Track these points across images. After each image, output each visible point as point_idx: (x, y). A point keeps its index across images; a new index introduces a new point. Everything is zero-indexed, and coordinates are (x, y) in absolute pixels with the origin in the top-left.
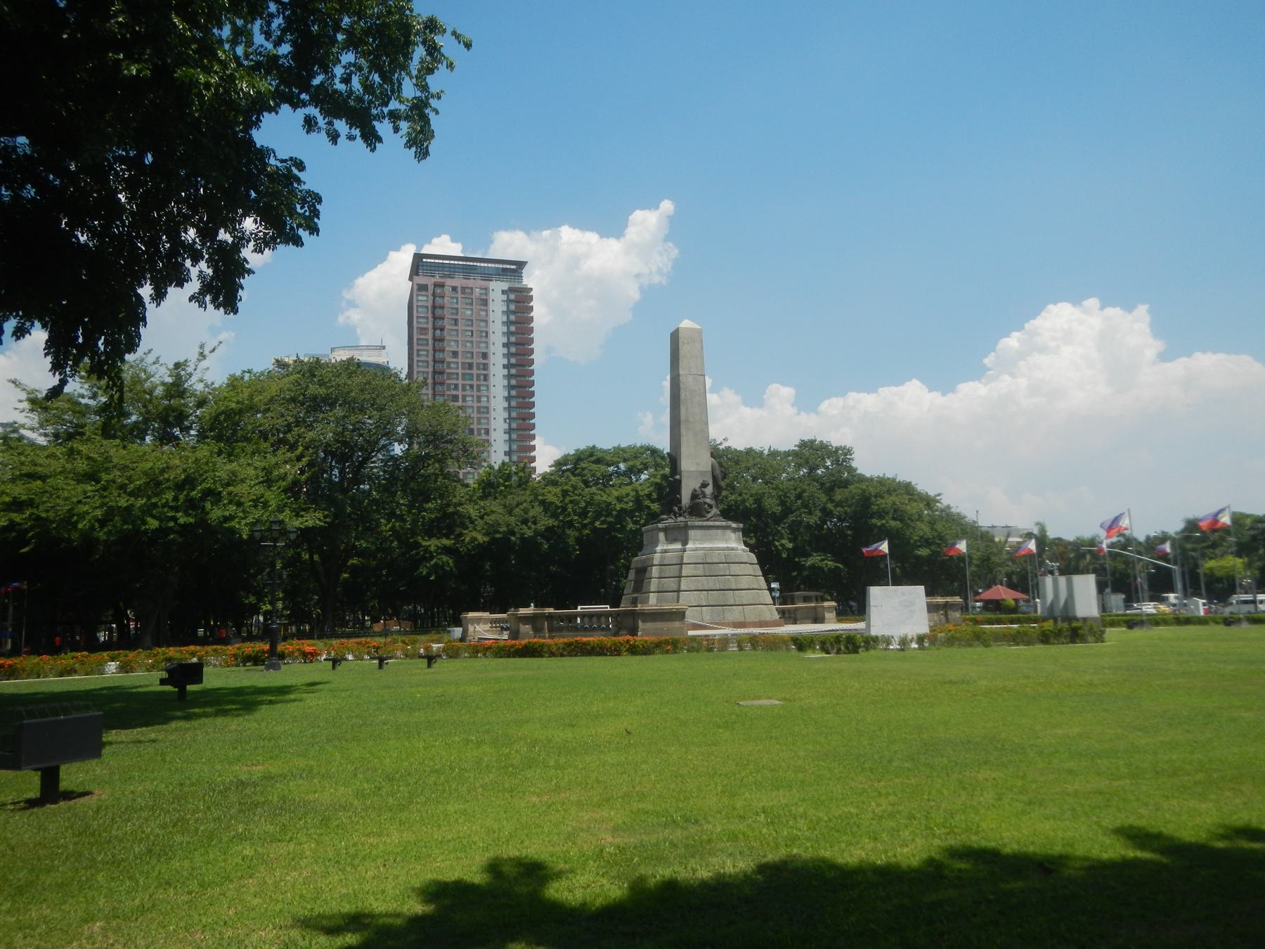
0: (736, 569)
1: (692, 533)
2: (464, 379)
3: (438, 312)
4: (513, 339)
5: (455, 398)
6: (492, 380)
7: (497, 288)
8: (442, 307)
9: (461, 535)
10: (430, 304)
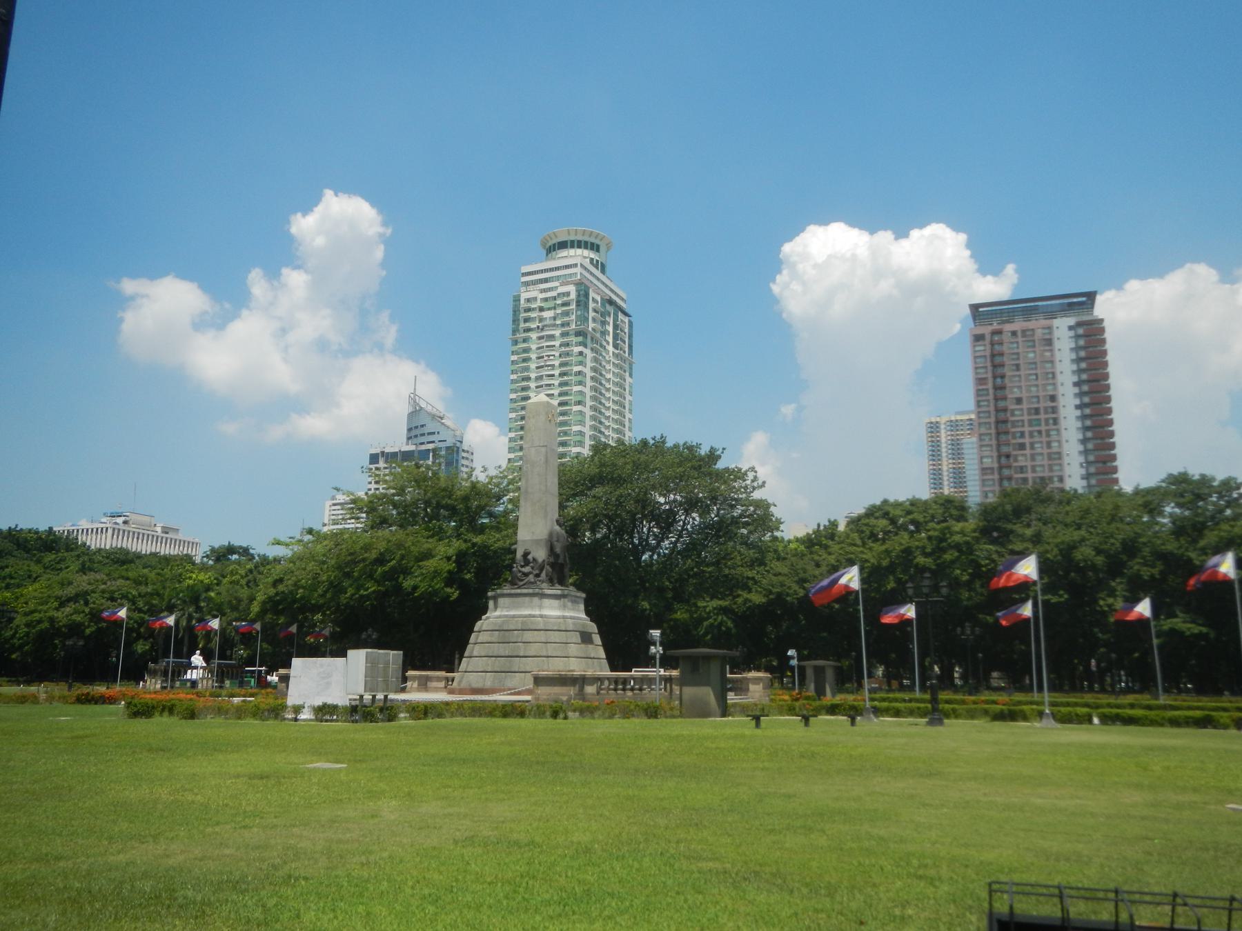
0: (528, 636)
1: (501, 601)
2: (1030, 425)
3: (998, 360)
4: (1084, 377)
5: (1022, 446)
6: (1063, 424)
7: (1062, 327)
8: (1002, 354)
9: (739, 596)
10: (988, 353)
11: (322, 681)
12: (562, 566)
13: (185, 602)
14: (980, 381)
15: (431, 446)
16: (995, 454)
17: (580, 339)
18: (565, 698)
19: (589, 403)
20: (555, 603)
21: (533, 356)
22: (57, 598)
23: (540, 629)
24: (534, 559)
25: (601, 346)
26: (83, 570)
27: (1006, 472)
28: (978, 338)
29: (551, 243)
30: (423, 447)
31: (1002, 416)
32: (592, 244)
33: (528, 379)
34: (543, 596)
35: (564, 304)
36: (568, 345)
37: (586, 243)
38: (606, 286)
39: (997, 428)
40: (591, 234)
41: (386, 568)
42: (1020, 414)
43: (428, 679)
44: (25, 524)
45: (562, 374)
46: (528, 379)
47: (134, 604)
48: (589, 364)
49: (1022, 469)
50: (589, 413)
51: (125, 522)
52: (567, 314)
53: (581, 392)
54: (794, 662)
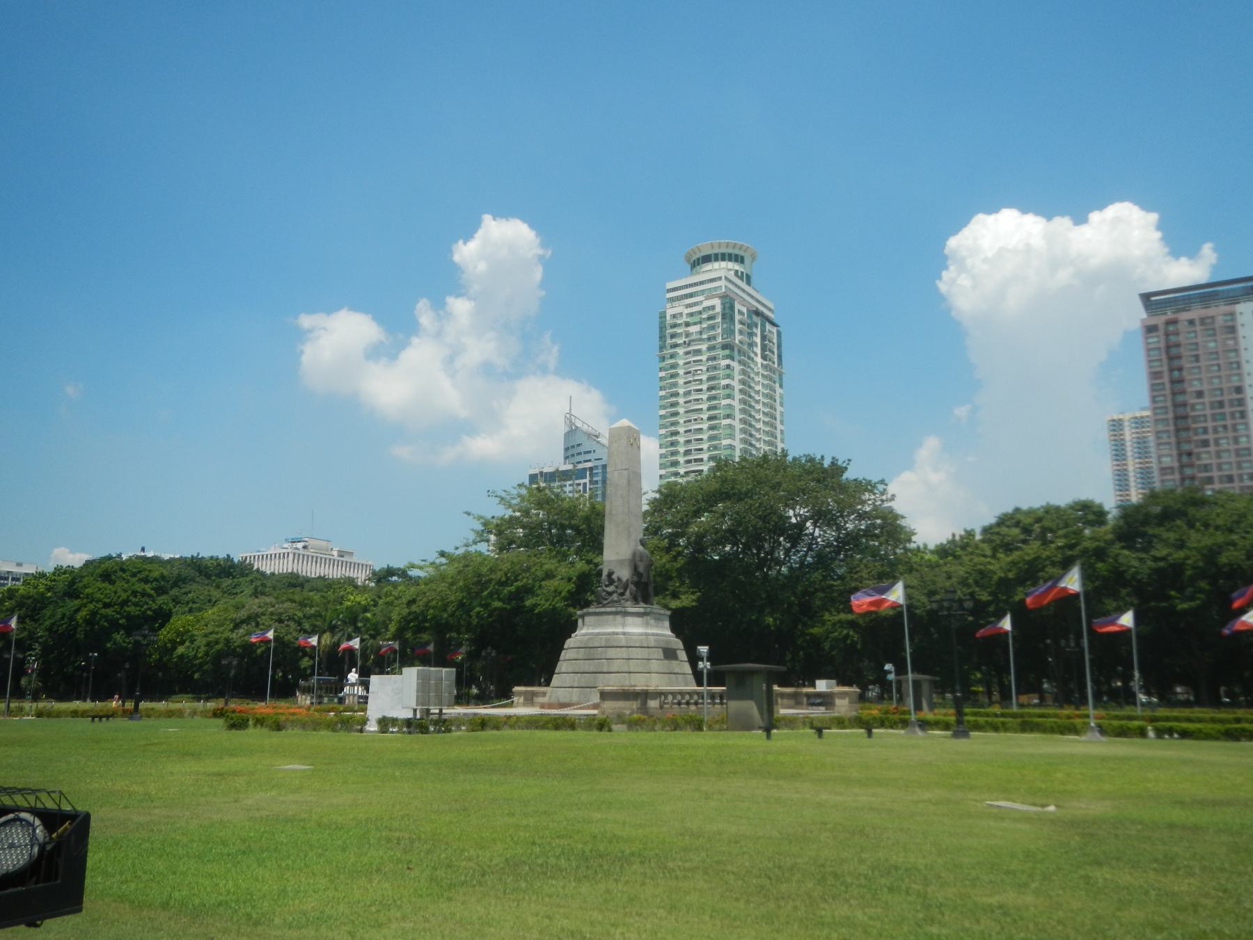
0: (612, 653)
1: (587, 619)
3: (1174, 351)
5: (1205, 443)
10: (1162, 345)
11: (393, 694)
12: (646, 585)
13: (344, 622)
14: (1155, 375)
15: (589, 465)
16: (1175, 452)
17: (727, 352)
18: (628, 712)
19: (738, 416)
20: (638, 620)
21: (681, 372)
22: (232, 620)
23: (627, 645)
24: (619, 579)
25: (749, 358)
26: (256, 594)
27: (1188, 471)
28: (1150, 329)
29: (695, 258)
30: (580, 466)
31: (1181, 411)
32: (737, 256)
33: (677, 394)
34: (626, 614)
35: (710, 318)
36: (714, 358)
37: (730, 255)
38: (752, 297)
39: (1176, 425)
40: (735, 246)
41: (513, 589)
42: (1202, 408)
43: (534, 694)
44: (206, 553)
45: (710, 389)
46: (677, 394)
47: (300, 624)
48: (738, 377)
49: (1206, 468)
50: (738, 426)
51: (305, 547)
52: (712, 327)
53: (730, 406)
54: (891, 677)
